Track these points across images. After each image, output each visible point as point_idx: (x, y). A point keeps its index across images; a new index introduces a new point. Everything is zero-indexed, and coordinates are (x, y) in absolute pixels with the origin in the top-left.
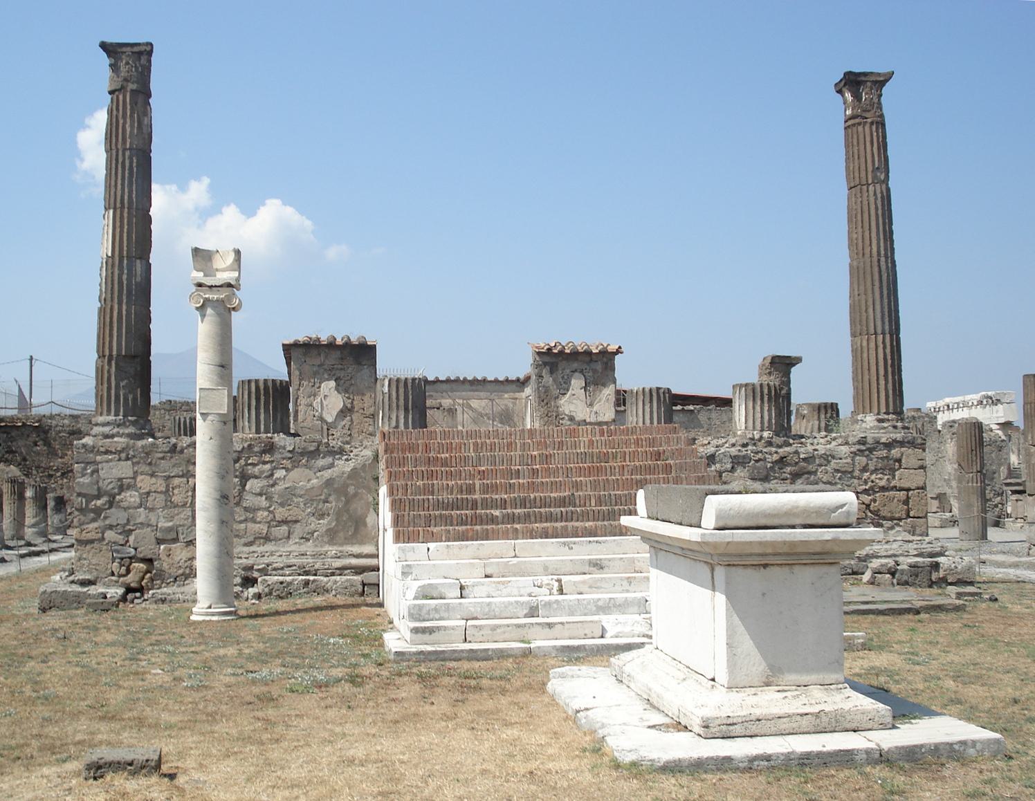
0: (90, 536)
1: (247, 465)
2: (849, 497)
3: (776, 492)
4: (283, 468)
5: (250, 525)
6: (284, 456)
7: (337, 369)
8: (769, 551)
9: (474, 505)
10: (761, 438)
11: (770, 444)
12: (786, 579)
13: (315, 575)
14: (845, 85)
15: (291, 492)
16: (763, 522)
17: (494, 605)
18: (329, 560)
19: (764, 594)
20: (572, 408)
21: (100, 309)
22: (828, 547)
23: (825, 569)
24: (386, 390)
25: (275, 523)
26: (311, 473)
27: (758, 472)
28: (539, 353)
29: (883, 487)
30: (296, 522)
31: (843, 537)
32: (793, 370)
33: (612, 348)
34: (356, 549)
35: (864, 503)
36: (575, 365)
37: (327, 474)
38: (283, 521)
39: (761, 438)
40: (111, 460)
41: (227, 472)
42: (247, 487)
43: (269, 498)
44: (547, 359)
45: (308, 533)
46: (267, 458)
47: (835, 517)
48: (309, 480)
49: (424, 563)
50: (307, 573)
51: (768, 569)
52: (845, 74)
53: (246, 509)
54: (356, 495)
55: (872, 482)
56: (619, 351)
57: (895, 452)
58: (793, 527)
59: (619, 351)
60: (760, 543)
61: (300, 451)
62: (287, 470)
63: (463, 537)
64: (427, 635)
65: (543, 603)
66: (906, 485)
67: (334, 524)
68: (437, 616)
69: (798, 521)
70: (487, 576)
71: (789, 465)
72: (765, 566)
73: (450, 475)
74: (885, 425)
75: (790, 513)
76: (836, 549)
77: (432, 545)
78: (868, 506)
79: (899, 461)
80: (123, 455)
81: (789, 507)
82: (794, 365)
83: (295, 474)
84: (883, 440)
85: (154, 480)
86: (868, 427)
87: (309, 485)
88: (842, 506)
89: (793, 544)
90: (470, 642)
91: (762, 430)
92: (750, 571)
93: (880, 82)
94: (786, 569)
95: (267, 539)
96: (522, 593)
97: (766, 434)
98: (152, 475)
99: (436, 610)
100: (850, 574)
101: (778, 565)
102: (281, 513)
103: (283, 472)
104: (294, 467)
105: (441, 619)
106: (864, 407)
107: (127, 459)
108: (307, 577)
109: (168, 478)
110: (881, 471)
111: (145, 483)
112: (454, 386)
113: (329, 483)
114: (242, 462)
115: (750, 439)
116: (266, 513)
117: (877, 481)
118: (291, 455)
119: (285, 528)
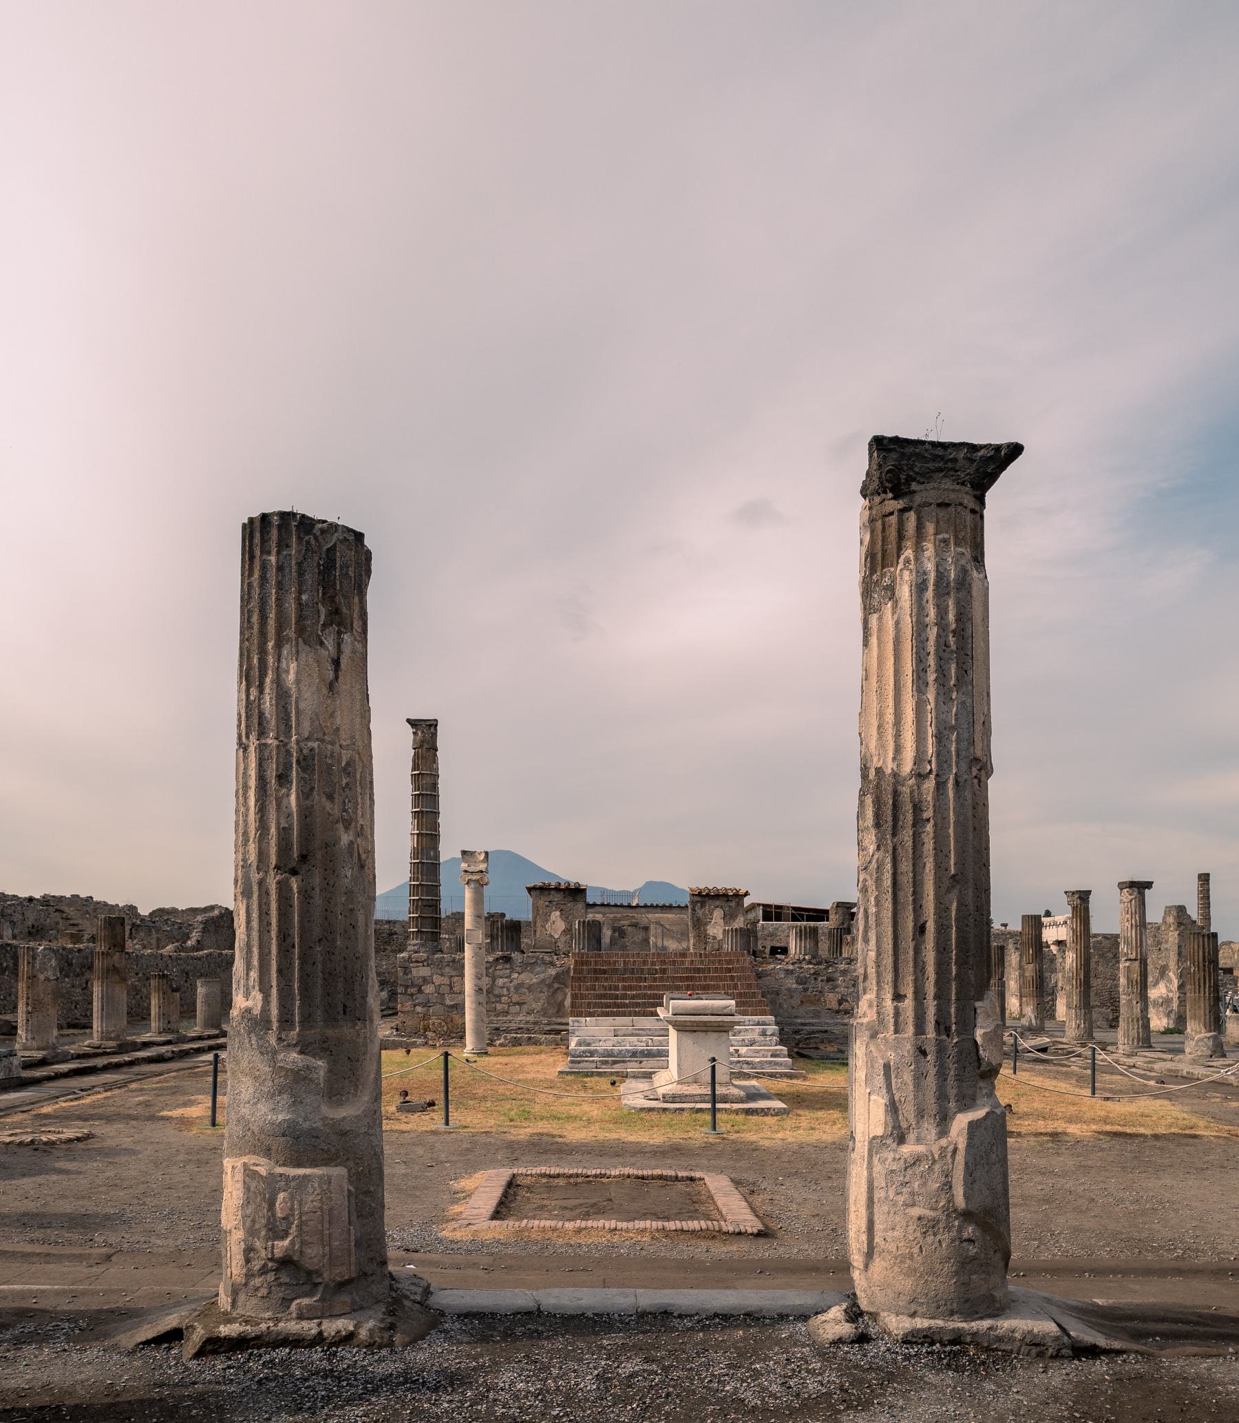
1: (496, 970)
2: (733, 1002)
5: (497, 1005)
9: (617, 997)
10: (804, 959)
11: (810, 963)
20: (715, 931)
22: (721, 1024)
23: (721, 1034)
24: (577, 927)
28: (693, 895)
30: (524, 1003)
33: (742, 892)
34: (559, 1020)
36: (718, 903)
37: (542, 976)
39: (804, 959)
40: (418, 967)
44: (698, 899)
47: (725, 1011)
53: (497, 996)
54: (558, 988)
59: (746, 894)
62: (519, 973)
63: (607, 1015)
69: (709, 1012)
72: (695, 1031)
73: (606, 979)
75: (705, 1008)
77: (588, 1019)
80: (425, 964)
83: (523, 976)
91: (805, 955)
95: (507, 1013)
97: (807, 957)
98: (442, 975)
102: (515, 998)
104: (523, 972)
107: (428, 965)
109: (451, 976)
111: (437, 980)
112: (650, 910)
113: (543, 981)
114: (493, 968)
116: (507, 998)
119: (517, 1007)
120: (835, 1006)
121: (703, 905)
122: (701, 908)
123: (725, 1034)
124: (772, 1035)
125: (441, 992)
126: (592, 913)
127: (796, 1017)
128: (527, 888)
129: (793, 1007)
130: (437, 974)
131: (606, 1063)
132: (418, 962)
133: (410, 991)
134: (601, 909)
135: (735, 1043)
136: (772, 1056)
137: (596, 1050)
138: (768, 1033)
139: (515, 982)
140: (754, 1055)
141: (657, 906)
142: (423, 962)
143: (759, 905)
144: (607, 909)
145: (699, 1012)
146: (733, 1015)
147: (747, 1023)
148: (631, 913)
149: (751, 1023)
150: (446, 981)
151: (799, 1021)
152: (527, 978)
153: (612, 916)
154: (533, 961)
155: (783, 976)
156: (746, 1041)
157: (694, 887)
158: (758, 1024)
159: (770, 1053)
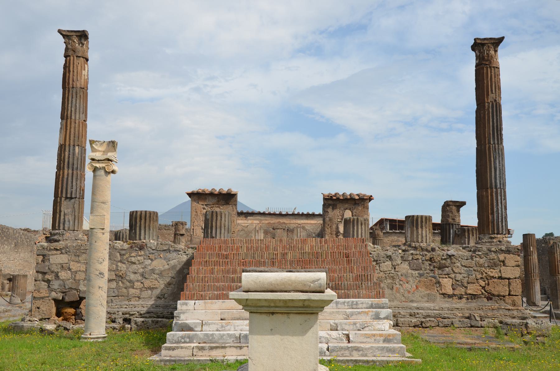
0: (42, 295)
2: (322, 275)
3: (301, 272)
4: (150, 259)
6: (150, 252)
7: (216, 207)
8: (272, 305)
12: (285, 321)
13: (163, 318)
14: (475, 46)
15: (153, 271)
16: (271, 288)
17: (215, 335)
18: (171, 310)
19: (271, 330)
21: (57, 172)
22: (306, 303)
25: (144, 289)
26: (165, 261)
27: (416, 266)
29: (493, 277)
30: (156, 288)
31: (313, 298)
32: (462, 209)
35: (481, 286)
36: (347, 206)
37: (172, 263)
38: (148, 288)
41: (104, 260)
42: (130, 269)
43: (142, 275)
44: (330, 202)
45: (161, 295)
46: (143, 253)
48: (164, 265)
49: (192, 311)
50: (158, 317)
51: (274, 315)
52: (84, 31)
53: (130, 281)
55: (486, 273)
56: (370, 199)
57: (502, 257)
58: (289, 291)
60: (266, 300)
61: (159, 249)
62: (152, 260)
64: (171, 351)
65: (242, 335)
66: (507, 276)
67: (176, 290)
68: (183, 340)
69: (291, 288)
70: (221, 319)
71: (435, 262)
72: (273, 313)
74: (495, 240)
76: (312, 305)
77: (197, 301)
78: (483, 288)
79: (503, 262)
80: (63, 251)
81: (286, 280)
82: (462, 206)
83: (155, 263)
84: (493, 249)
85: (79, 265)
86: (484, 241)
87: (163, 269)
88: (318, 280)
89: (285, 301)
90: (195, 355)
92: (264, 316)
93: (497, 42)
94: (286, 315)
96: (236, 329)
98: (78, 262)
99: (182, 337)
100: (469, 327)
101: (280, 313)
102: (147, 283)
103: (150, 261)
105: (185, 342)
106: (150, 217)
108: (158, 319)
110: (492, 267)
112: (297, 217)
113: (173, 267)
114: (127, 255)
115: (413, 247)
116: (139, 284)
117: (490, 273)
118: (153, 252)
119: (150, 292)
120: (450, 291)
121: (334, 207)
122: (333, 209)
123: (313, 317)
124: (386, 318)
125: (77, 278)
126: (251, 220)
127: (412, 301)
128: (188, 194)
129: (409, 292)
130: (73, 261)
131: (202, 349)
132: (57, 250)
133: (47, 277)
134: (259, 217)
135: (347, 327)
136: (384, 341)
137: (196, 334)
138: (382, 316)
139: (150, 268)
140: (365, 340)
141: (303, 215)
142: (61, 249)
143: (386, 220)
144: (262, 218)
145: (278, 288)
146: (323, 292)
147: (360, 306)
148: (282, 220)
149: (364, 306)
150: (83, 268)
151: (415, 305)
152: (159, 264)
153: (267, 222)
154: (165, 248)
155: (399, 262)
156: (358, 325)
157: (326, 193)
158: (371, 307)
159: (382, 338)
